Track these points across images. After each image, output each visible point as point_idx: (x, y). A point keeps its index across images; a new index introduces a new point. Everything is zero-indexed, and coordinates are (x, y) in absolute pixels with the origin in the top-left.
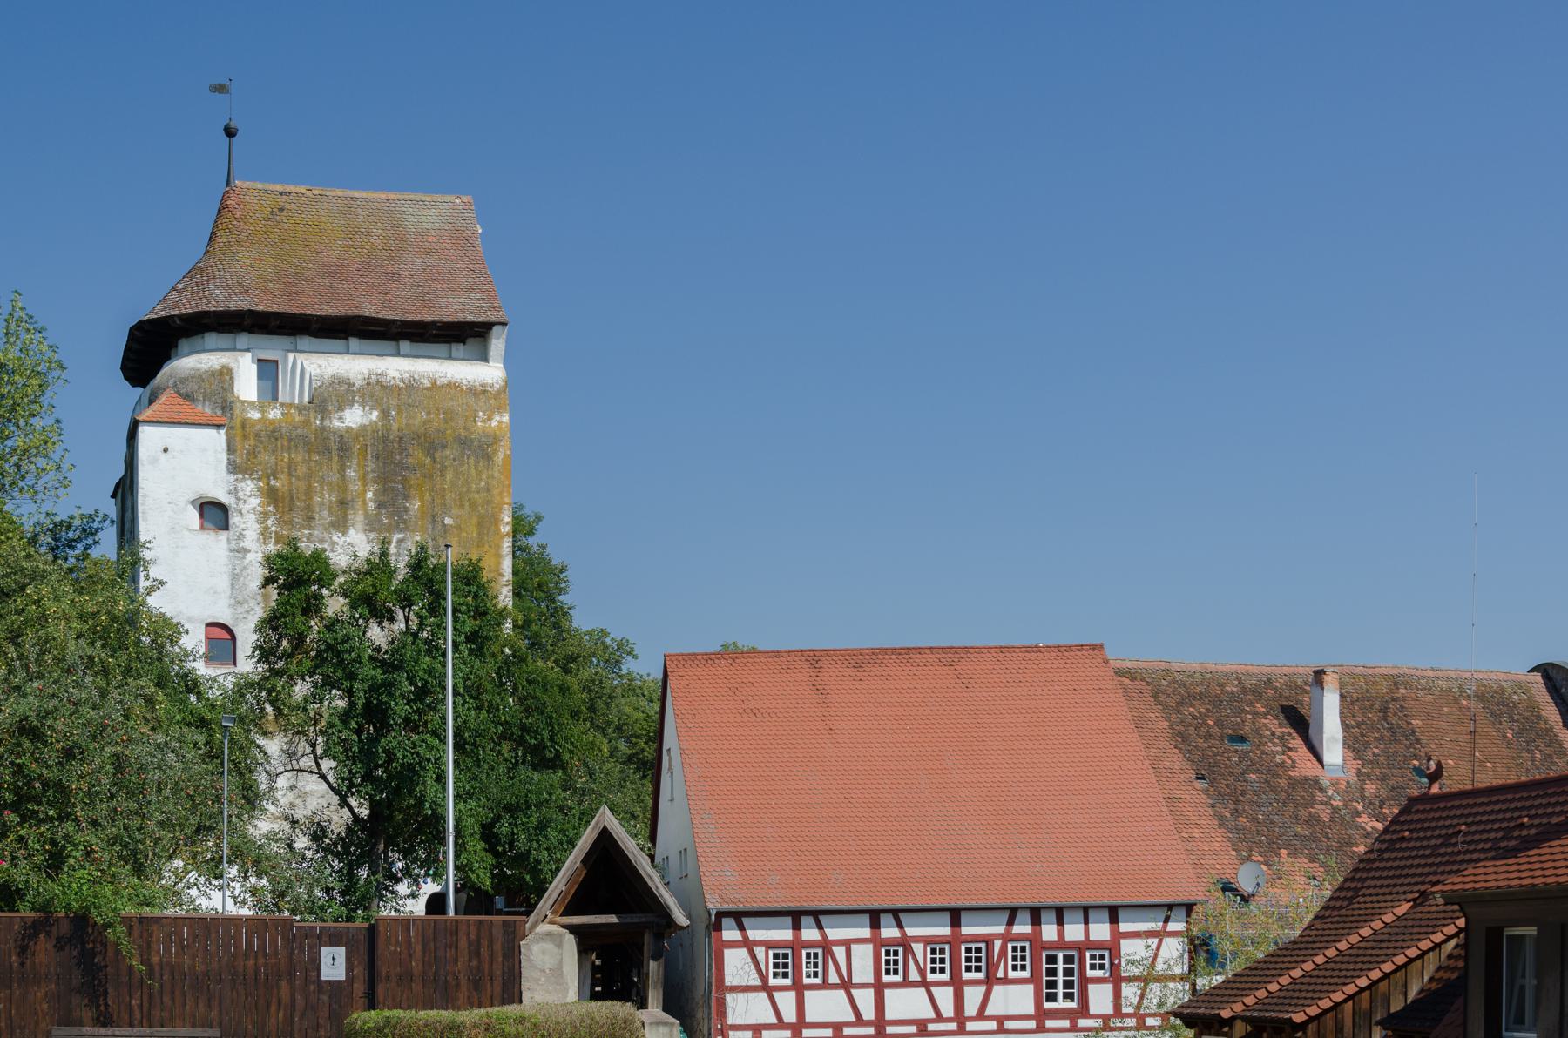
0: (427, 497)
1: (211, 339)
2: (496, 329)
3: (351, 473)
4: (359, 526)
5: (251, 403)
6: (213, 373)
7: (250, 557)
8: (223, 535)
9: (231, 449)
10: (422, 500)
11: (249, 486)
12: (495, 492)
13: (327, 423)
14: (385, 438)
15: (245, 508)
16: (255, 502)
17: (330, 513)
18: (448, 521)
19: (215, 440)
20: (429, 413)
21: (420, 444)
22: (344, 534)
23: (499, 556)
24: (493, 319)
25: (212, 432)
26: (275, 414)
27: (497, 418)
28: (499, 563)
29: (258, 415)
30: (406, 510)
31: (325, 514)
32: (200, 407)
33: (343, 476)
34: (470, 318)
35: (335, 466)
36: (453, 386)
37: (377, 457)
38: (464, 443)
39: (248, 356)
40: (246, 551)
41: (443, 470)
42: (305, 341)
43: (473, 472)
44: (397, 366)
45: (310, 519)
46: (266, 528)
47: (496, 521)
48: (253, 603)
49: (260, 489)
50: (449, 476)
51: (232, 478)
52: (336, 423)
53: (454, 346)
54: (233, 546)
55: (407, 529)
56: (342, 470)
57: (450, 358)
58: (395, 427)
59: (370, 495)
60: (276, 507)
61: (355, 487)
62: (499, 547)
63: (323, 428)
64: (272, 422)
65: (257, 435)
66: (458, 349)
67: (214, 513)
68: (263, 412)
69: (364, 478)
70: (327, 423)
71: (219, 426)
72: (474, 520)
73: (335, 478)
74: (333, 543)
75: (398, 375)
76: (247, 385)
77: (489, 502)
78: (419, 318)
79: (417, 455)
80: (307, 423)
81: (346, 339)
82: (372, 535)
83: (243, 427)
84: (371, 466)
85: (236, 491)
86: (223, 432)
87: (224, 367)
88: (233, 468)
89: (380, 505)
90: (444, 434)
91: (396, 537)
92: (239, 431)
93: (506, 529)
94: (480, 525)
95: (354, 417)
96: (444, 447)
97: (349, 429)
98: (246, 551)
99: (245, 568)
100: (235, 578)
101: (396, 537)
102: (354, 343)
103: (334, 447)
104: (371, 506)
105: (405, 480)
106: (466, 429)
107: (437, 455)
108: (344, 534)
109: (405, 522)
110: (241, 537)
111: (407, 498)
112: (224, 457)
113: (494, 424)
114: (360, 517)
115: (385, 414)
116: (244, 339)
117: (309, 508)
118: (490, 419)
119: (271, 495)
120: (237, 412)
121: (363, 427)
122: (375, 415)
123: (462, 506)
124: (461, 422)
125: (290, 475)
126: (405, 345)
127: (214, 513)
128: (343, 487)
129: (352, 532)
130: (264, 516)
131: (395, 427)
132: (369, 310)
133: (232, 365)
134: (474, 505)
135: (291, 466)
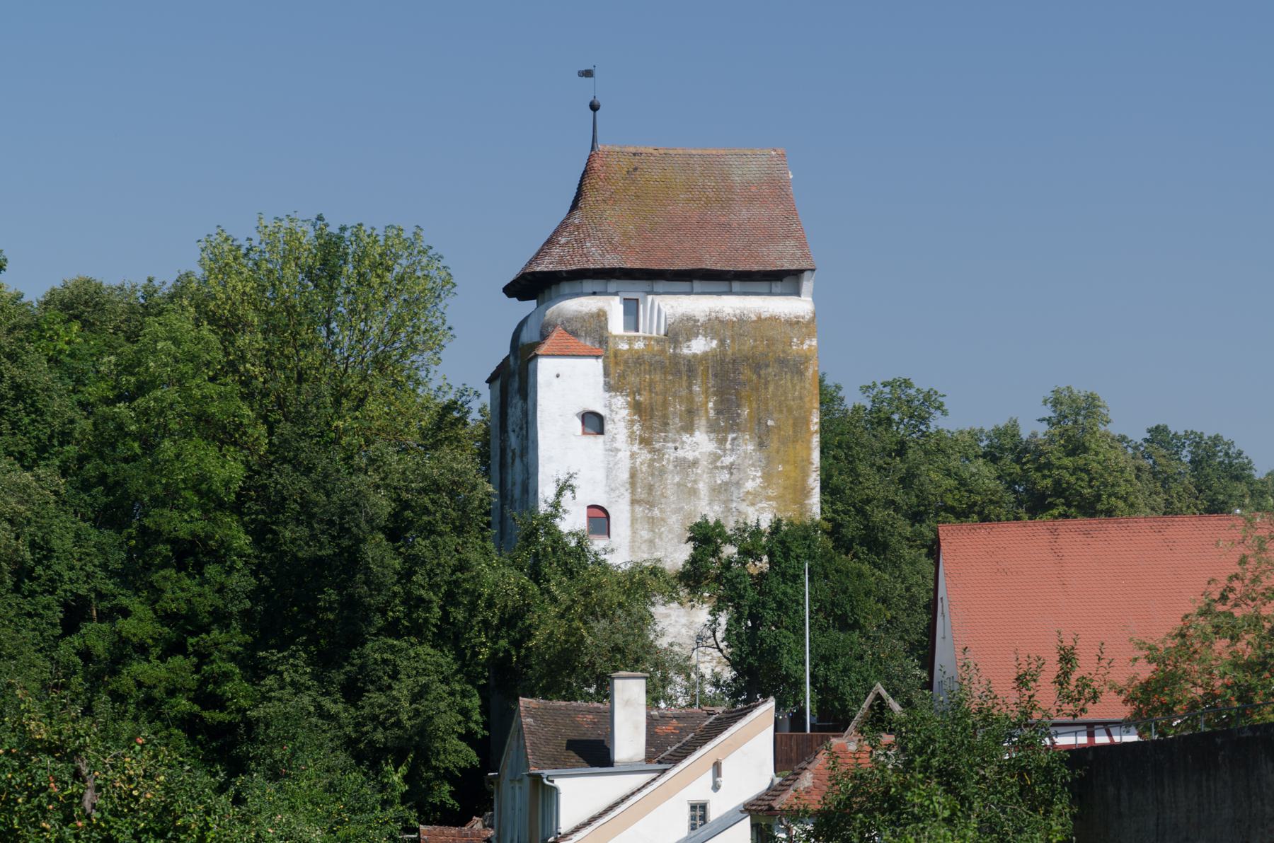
0: (754, 405)
1: (588, 285)
2: (806, 274)
3: (696, 388)
4: (703, 429)
5: (621, 338)
6: (592, 316)
7: (620, 454)
8: (601, 438)
9: (606, 374)
10: (750, 408)
11: (620, 401)
12: (807, 400)
13: (678, 351)
14: (722, 361)
15: (617, 418)
16: (625, 413)
17: (681, 420)
18: (770, 423)
19: (596, 366)
20: (755, 341)
21: (749, 365)
22: (691, 435)
23: (809, 449)
24: (803, 265)
25: (592, 361)
26: (639, 345)
27: (808, 342)
28: (809, 455)
29: (626, 347)
30: (739, 415)
31: (677, 420)
32: (582, 341)
33: (691, 391)
34: (787, 266)
35: (685, 384)
36: (774, 319)
37: (716, 376)
38: (783, 362)
39: (617, 299)
40: (617, 450)
41: (767, 383)
42: (660, 285)
43: (789, 384)
44: (731, 305)
45: (666, 424)
46: (633, 432)
47: (807, 422)
48: (622, 490)
49: (628, 403)
50: (771, 388)
51: (607, 395)
52: (685, 351)
53: (774, 284)
54: (608, 447)
55: (739, 430)
56: (690, 386)
57: (770, 294)
58: (730, 352)
59: (711, 405)
60: (640, 416)
61: (699, 399)
62: (809, 442)
63: (675, 355)
64: (637, 352)
65: (626, 362)
66: (777, 286)
67: (593, 422)
68: (630, 344)
69: (706, 392)
70: (678, 351)
71: (597, 357)
72: (791, 422)
73: (684, 393)
74: (683, 442)
75: (731, 311)
76: (616, 324)
77: (801, 408)
78: (747, 268)
79: (747, 373)
80: (663, 351)
81: (691, 281)
82: (712, 435)
83: (616, 356)
84: (711, 382)
85: (610, 405)
86: (600, 361)
87: (600, 310)
88: (609, 387)
89: (718, 412)
90: (767, 356)
91: (730, 436)
92: (612, 359)
93: (815, 427)
94: (795, 425)
95: (699, 346)
96: (767, 366)
97: (695, 355)
98: (617, 450)
99: (616, 464)
100: (609, 471)
101: (730, 436)
102: (697, 285)
103: (684, 369)
104: (712, 413)
105: (737, 393)
106: (784, 352)
107: (762, 372)
108: (691, 435)
109: (737, 425)
110: (614, 439)
111: (739, 406)
112: (601, 379)
113: (805, 347)
114: (703, 422)
115: (722, 342)
116: (613, 285)
117: (665, 416)
118: (802, 343)
119: (637, 408)
120: (611, 344)
121: (706, 354)
122: (714, 343)
123: (781, 411)
124: (781, 347)
125: (651, 391)
126: (736, 285)
127: (593, 422)
128: (690, 399)
129: (697, 433)
130: (632, 422)
131: (730, 352)
132: (710, 263)
133: (606, 308)
134: (790, 410)
135: (651, 384)
